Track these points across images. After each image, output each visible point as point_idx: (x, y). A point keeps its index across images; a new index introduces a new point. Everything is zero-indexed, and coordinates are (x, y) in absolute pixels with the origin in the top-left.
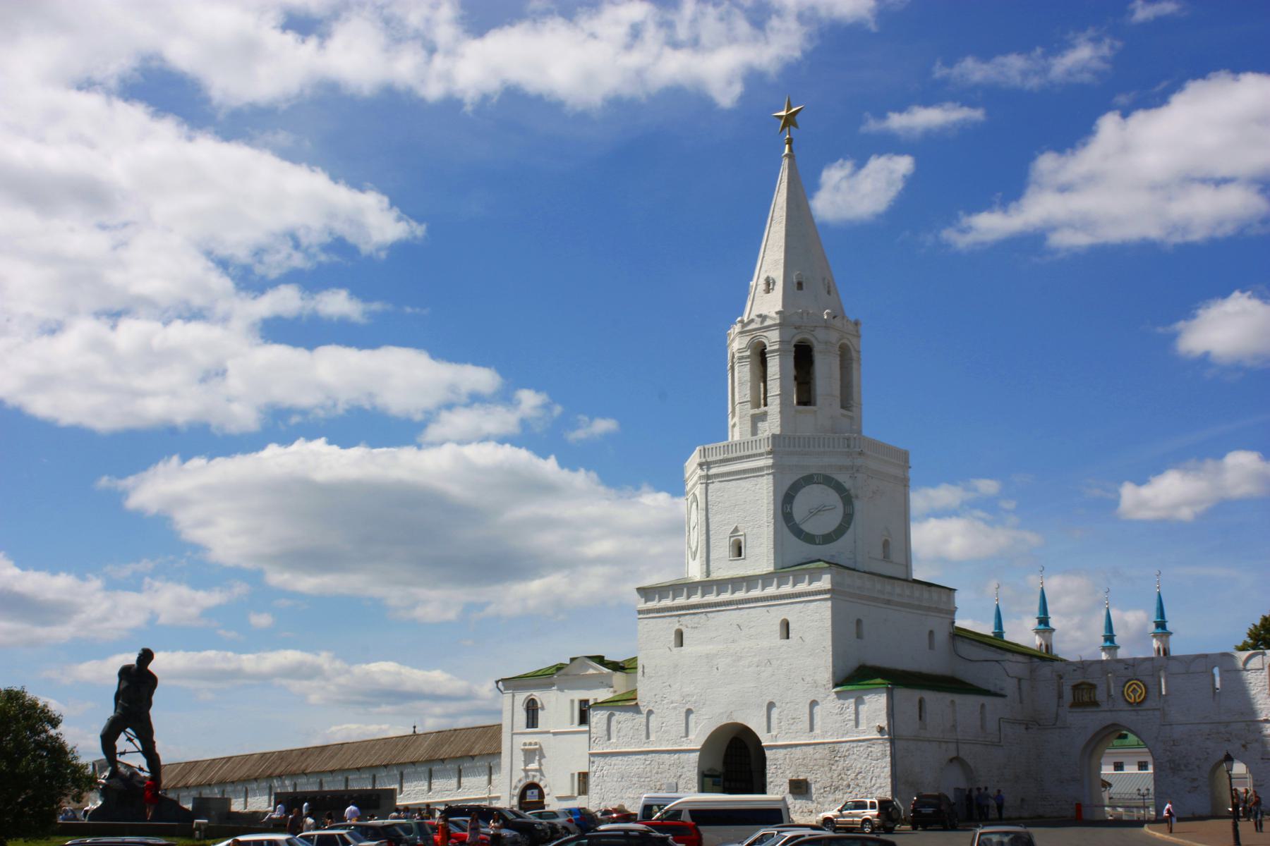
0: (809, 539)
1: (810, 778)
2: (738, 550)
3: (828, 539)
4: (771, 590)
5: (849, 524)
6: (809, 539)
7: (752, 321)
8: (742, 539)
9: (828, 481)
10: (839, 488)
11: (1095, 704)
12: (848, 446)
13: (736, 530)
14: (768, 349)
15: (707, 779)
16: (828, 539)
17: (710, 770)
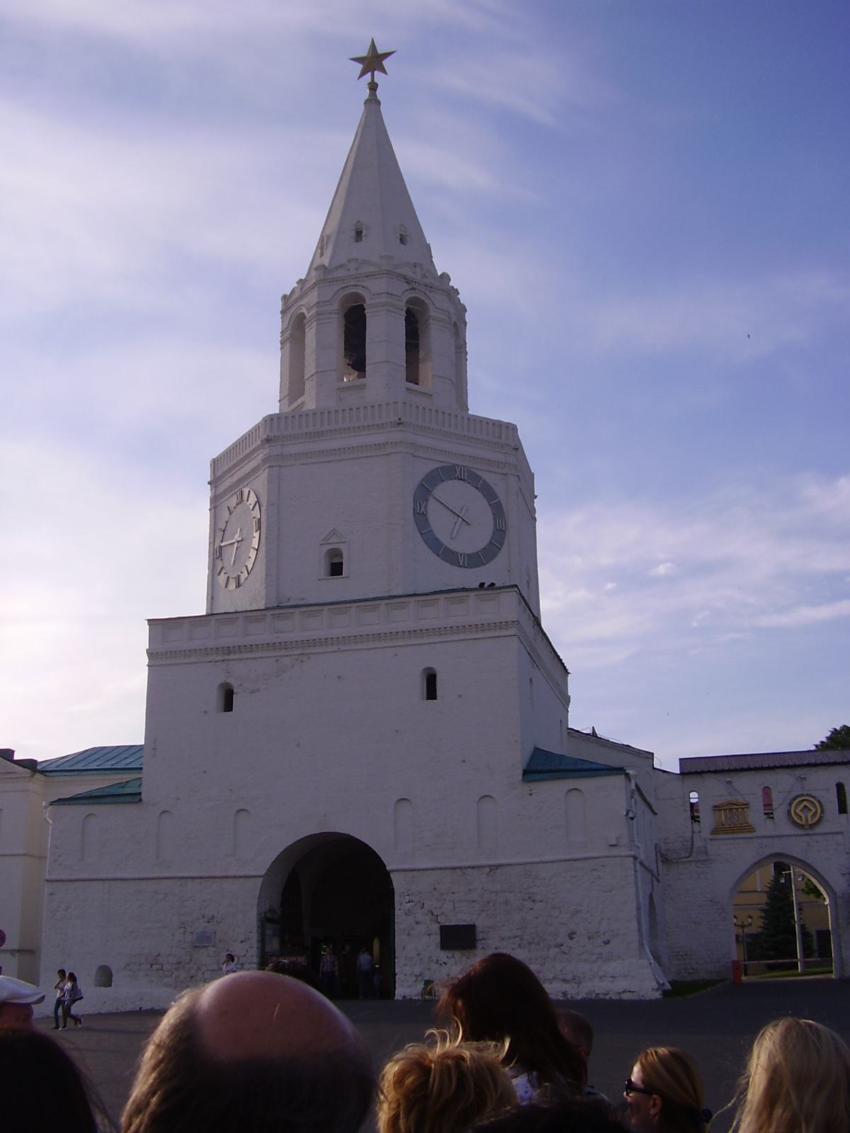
0: (451, 557)
1: (481, 923)
2: (336, 569)
3: (475, 560)
4: (405, 619)
5: (502, 544)
6: (451, 557)
7: (342, 266)
8: (343, 547)
9: (473, 479)
10: (488, 492)
11: (751, 829)
12: (500, 437)
13: (334, 532)
14: (368, 301)
15: (268, 925)
16: (475, 560)
17: (271, 910)
